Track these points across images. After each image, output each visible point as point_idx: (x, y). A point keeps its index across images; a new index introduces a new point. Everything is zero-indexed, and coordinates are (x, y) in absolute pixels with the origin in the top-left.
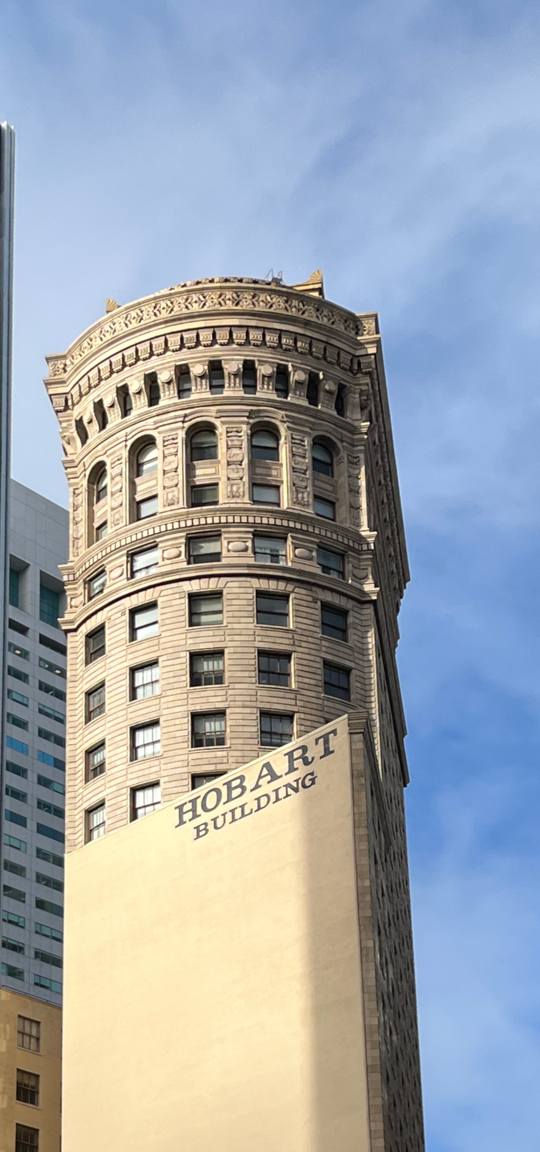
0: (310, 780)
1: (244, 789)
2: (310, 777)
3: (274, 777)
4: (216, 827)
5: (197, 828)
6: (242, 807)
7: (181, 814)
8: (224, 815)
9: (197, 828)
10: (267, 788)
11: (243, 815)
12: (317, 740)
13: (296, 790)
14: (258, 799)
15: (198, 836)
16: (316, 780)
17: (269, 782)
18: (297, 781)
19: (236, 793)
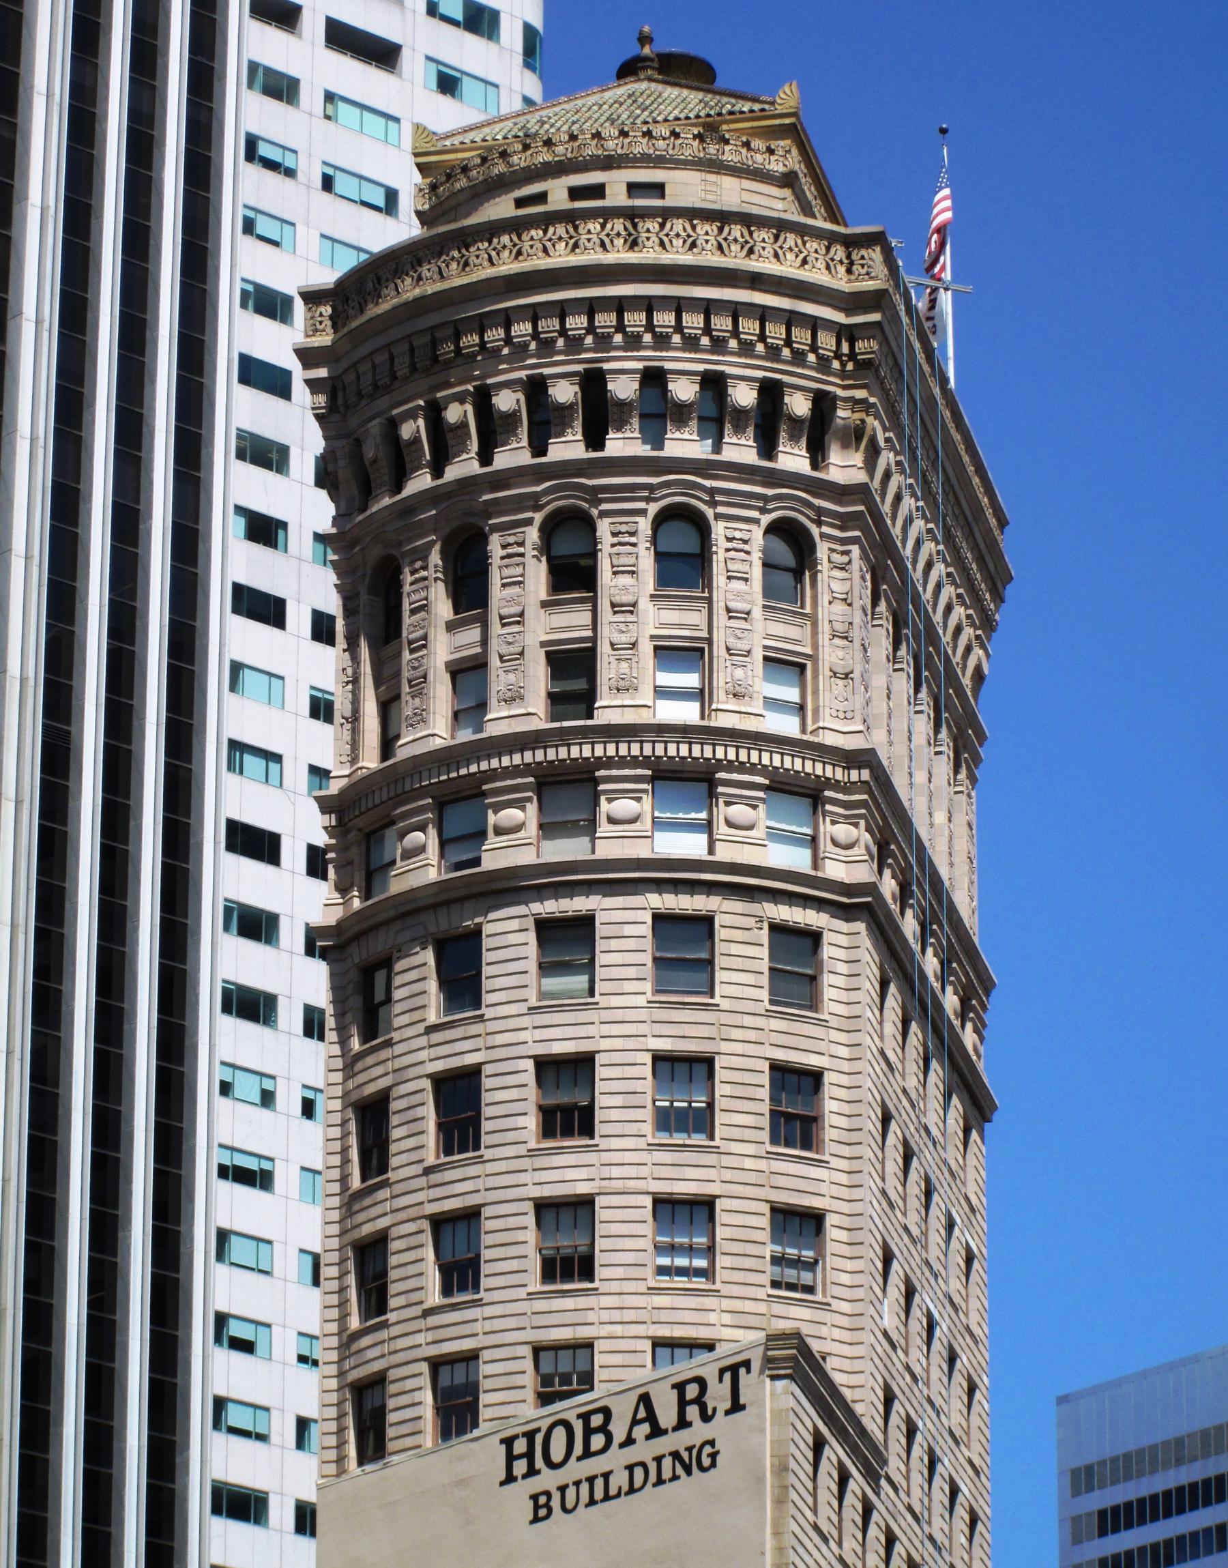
0: (709, 1455)
3: (657, 1432)
5: (534, 1498)
6: (606, 1476)
7: (511, 1458)
9: (534, 1498)
10: (644, 1450)
12: (722, 1372)
13: (688, 1471)
14: (630, 1468)
16: (719, 1458)
17: (648, 1438)
18: (689, 1449)
19: (597, 1441)
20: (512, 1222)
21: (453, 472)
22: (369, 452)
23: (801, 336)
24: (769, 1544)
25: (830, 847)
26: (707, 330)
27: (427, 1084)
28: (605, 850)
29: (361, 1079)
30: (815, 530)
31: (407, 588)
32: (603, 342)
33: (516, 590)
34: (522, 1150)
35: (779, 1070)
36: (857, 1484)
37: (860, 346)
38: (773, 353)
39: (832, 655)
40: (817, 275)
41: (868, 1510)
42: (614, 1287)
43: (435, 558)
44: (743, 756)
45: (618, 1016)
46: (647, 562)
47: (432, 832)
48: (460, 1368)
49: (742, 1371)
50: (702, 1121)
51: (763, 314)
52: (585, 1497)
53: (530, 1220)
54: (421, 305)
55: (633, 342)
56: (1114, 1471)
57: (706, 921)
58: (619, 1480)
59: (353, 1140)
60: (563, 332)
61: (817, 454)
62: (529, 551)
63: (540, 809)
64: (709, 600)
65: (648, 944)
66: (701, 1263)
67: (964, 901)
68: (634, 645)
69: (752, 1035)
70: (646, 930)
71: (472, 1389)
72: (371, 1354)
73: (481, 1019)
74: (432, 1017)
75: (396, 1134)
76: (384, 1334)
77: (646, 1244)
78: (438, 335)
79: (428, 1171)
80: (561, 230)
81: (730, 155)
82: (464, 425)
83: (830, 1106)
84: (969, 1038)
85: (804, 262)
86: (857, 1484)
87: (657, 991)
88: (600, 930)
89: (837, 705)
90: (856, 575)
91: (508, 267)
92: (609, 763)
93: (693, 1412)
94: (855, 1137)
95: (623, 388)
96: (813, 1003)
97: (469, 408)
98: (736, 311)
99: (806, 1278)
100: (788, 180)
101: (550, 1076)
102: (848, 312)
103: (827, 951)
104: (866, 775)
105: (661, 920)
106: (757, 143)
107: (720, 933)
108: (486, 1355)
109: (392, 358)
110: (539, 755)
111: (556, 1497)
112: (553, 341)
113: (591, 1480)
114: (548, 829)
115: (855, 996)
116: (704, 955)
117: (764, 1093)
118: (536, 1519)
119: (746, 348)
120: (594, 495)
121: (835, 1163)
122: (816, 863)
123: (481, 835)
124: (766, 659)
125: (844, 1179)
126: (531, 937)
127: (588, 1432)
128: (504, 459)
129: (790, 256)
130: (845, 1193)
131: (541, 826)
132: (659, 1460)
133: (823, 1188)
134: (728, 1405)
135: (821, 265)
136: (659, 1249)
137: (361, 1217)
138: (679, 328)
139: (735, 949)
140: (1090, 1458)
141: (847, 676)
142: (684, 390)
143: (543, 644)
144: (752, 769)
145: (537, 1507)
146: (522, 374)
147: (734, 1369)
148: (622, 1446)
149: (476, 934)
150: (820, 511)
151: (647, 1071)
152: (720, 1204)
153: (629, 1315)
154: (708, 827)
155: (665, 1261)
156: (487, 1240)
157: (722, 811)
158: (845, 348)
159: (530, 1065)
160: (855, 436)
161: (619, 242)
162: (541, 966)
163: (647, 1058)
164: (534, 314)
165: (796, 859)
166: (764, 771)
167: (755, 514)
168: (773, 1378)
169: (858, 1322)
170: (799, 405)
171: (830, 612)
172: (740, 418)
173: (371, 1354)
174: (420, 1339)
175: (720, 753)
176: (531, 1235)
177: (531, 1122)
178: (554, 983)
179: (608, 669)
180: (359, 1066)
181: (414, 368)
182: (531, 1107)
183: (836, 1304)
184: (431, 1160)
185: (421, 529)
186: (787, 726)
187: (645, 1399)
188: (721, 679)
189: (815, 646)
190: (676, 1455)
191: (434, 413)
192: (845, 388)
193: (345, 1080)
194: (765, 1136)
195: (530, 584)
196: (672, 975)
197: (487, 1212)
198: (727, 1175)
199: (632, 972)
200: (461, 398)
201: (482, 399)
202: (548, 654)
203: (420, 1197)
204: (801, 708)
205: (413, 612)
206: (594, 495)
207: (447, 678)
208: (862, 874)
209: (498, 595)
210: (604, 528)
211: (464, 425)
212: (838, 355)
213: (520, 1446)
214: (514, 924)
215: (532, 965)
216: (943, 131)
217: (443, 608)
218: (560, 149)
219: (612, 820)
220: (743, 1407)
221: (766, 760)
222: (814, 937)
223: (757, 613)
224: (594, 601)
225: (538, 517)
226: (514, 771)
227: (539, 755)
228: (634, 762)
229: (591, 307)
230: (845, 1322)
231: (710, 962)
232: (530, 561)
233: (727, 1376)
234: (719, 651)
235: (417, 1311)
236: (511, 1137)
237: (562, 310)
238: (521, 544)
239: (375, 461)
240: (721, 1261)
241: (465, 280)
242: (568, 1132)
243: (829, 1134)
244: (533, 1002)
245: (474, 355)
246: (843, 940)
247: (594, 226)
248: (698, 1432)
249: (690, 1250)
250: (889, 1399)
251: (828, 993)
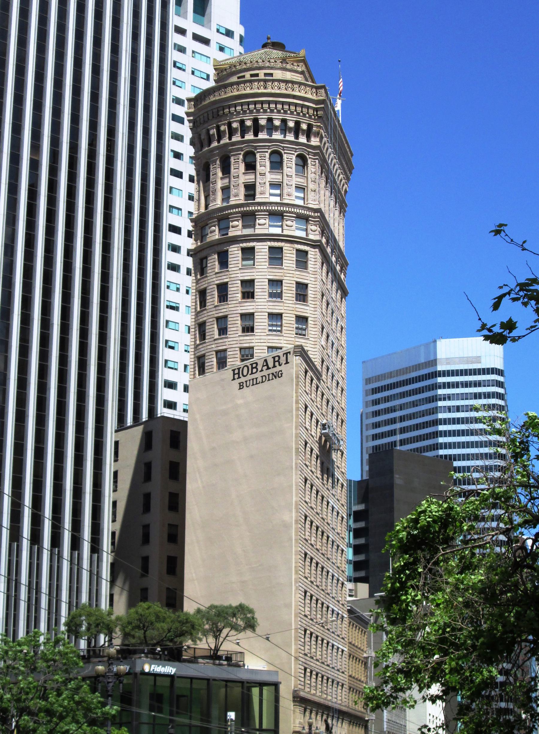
2: (280, 372)
3: (268, 368)
5: (240, 383)
6: (256, 379)
7: (234, 374)
9: (240, 383)
10: (265, 373)
12: (284, 354)
13: (276, 377)
14: (262, 377)
18: (276, 372)
19: (254, 370)
20: (235, 319)
21: (222, 142)
22: (203, 137)
23: (305, 110)
24: (294, 395)
25: (310, 231)
26: (283, 109)
27: (215, 286)
28: (258, 232)
29: (200, 285)
30: (308, 156)
31: (211, 169)
32: (258, 111)
33: (237, 170)
34: (237, 302)
35: (298, 284)
36: (315, 381)
37: (319, 113)
38: (298, 114)
39: (311, 186)
40: (309, 96)
41: (317, 387)
42: (259, 334)
43: (218, 162)
44: (290, 210)
45: (260, 270)
46: (268, 164)
47: (217, 227)
48: (222, 353)
50: (279, 295)
51: (296, 105)
52: (251, 384)
53: (239, 318)
54: (215, 102)
55: (265, 111)
56: (376, 379)
57: (281, 249)
58: (260, 380)
59: (198, 299)
60: (249, 109)
61: (308, 138)
62: (240, 161)
63: (242, 222)
64: (282, 173)
65: (267, 254)
66: (279, 329)
67: (341, 244)
68: (265, 183)
69: (291, 275)
70: (267, 250)
71: (225, 358)
72: (202, 349)
73: (228, 271)
74: (217, 270)
75: (208, 298)
76: (205, 345)
77: (267, 324)
78: (219, 109)
79: (216, 307)
80: (248, 84)
81: (288, 66)
82: (225, 131)
83: (309, 292)
84: (342, 276)
85: (306, 92)
86: (315, 381)
87: (269, 265)
88: (256, 250)
89: (312, 198)
90: (317, 168)
91: (236, 93)
92: (259, 211)
93: (277, 364)
94: (315, 299)
95: (263, 122)
96: (306, 268)
97: (226, 127)
98: (289, 104)
99: (304, 332)
100: (302, 73)
101: (244, 284)
102: (316, 105)
103: (309, 256)
104: (319, 214)
105: (270, 248)
106: (295, 64)
107: (284, 251)
108: (229, 350)
109: (208, 115)
110: (242, 209)
111: (245, 383)
112: (246, 111)
113: (253, 379)
114: (244, 227)
115: (316, 266)
116: (281, 256)
117: (294, 289)
118: (240, 389)
119: (292, 113)
120: (256, 148)
121: (311, 305)
122: (307, 235)
123: (229, 228)
124: (296, 187)
125: (313, 309)
126: (240, 252)
127: (252, 368)
128: (234, 139)
129: (303, 91)
130: (313, 313)
131: (242, 226)
132: (269, 375)
133: (308, 311)
134: (285, 362)
135: (310, 93)
136: (269, 325)
137: (199, 317)
138: (276, 108)
139: (288, 255)
140: (370, 376)
141: (315, 191)
142: (277, 123)
143: (243, 183)
144: (292, 213)
145: (240, 386)
146: (239, 119)
147: (286, 354)
148: (260, 371)
149: (227, 251)
150: (309, 152)
151: (267, 284)
152: (283, 315)
153: (262, 341)
154: (282, 226)
155: (271, 328)
156: (229, 323)
157: (285, 222)
158: (315, 113)
159: (239, 282)
160: (317, 134)
161: (262, 87)
162: (242, 259)
163: (267, 280)
164: (242, 104)
165: (302, 234)
166: (295, 213)
167: (293, 152)
168: (296, 356)
169: (316, 343)
170: (304, 127)
171: (311, 176)
172: (290, 129)
173: (202, 349)
174: (213, 346)
175: (285, 209)
176: (239, 322)
177: (240, 295)
178: (245, 263)
179: (258, 189)
180: (199, 282)
181: (213, 117)
182: (240, 292)
183: (311, 339)
184: (216, 304)
185: (214, 155)
186: (300, 203)
187: (266, 361)
188: (285, 191)
189: (307, 184)
190: (273, 374)
191: (218, 128)
192: (315, 123)
193: (196, 285)
194: (294, 299)
195: (240, 168)
196: (273, 261)
197: (229, 316)
198: (285, 308)
199: (263, 260)
200: (224, 124)
201: (229, 125)
202: (245, 185)
203: (214, 313)
204: (304, 199)
205: (213, 175)
206: (256, 148)
207: (221, 191)
208: (318, 238)
209: (233, 170)
210: (258, 155)
211: (225, 131)
212: (313, 115)
213: (236, 371)
214: (236, 249)
215: (240, 259)
216: (339, 61)
217: (220, 174)
218: (248, 65)
219: (259, 225)
220: (288, 363)
221: (295, 210)
222: (306, 252)
223: (294, 176)
224: (255, 173)
225: (242, 153)
226: (236, 213)
227: (242, 209)
228: (265, 211)
229: (255, 103)
230: (313, 343)
231: (282, 258)
232: (240, 163)
233: (285, 355)
234: (285, 184)
235: (212, 339)
236: (235, 299)
237: (248, 104)
238: (238, 159)
239: (204, 139)
240: (284, 328)
241: (226, 96)
242: (248, 298)
243: (309, 299)
244: (240, 267)
245: (227, 114)
246: (313, 253)
247: (256, 84)
248: (278, 368)
249: (277, 326)
250: (323, 361)
251: (309, 266)
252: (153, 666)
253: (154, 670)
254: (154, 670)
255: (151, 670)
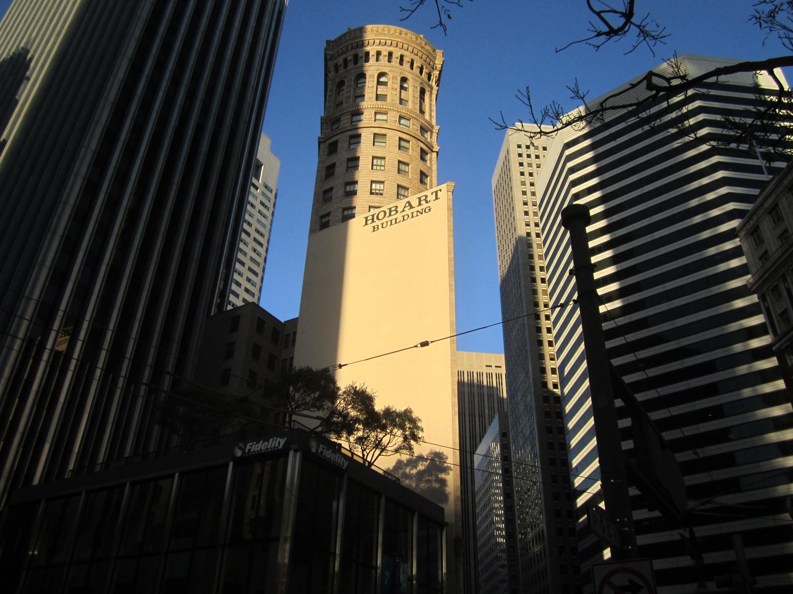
1: (397, 212)
2: (428, 208)
4: (382, 227)
5: (374, 227)
8: (387, 222)
11: (396, 223)
13: (422, 213)
15: (374, 231)
16: (431, 210)
49: (439, 192)
190: (418, 211)
236: (366, 168)
252: (321, 446)
253: (322, 452)
254: (322, 452)
255: (319, 452)
